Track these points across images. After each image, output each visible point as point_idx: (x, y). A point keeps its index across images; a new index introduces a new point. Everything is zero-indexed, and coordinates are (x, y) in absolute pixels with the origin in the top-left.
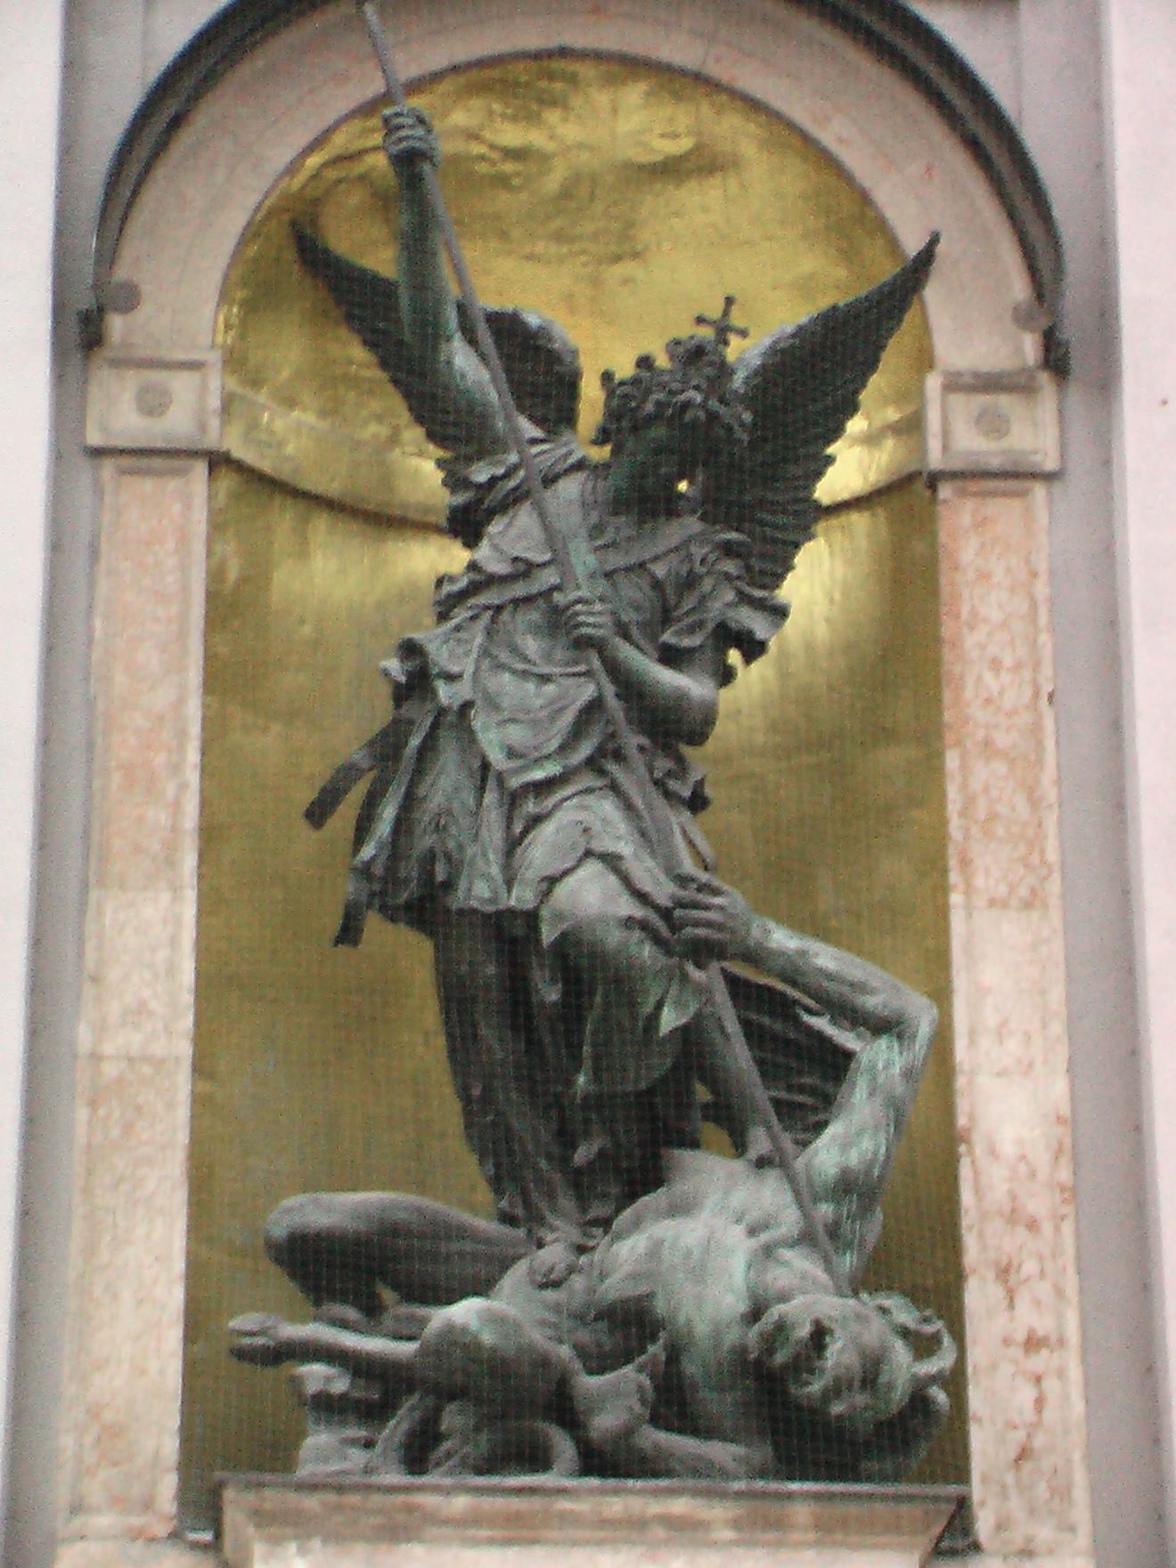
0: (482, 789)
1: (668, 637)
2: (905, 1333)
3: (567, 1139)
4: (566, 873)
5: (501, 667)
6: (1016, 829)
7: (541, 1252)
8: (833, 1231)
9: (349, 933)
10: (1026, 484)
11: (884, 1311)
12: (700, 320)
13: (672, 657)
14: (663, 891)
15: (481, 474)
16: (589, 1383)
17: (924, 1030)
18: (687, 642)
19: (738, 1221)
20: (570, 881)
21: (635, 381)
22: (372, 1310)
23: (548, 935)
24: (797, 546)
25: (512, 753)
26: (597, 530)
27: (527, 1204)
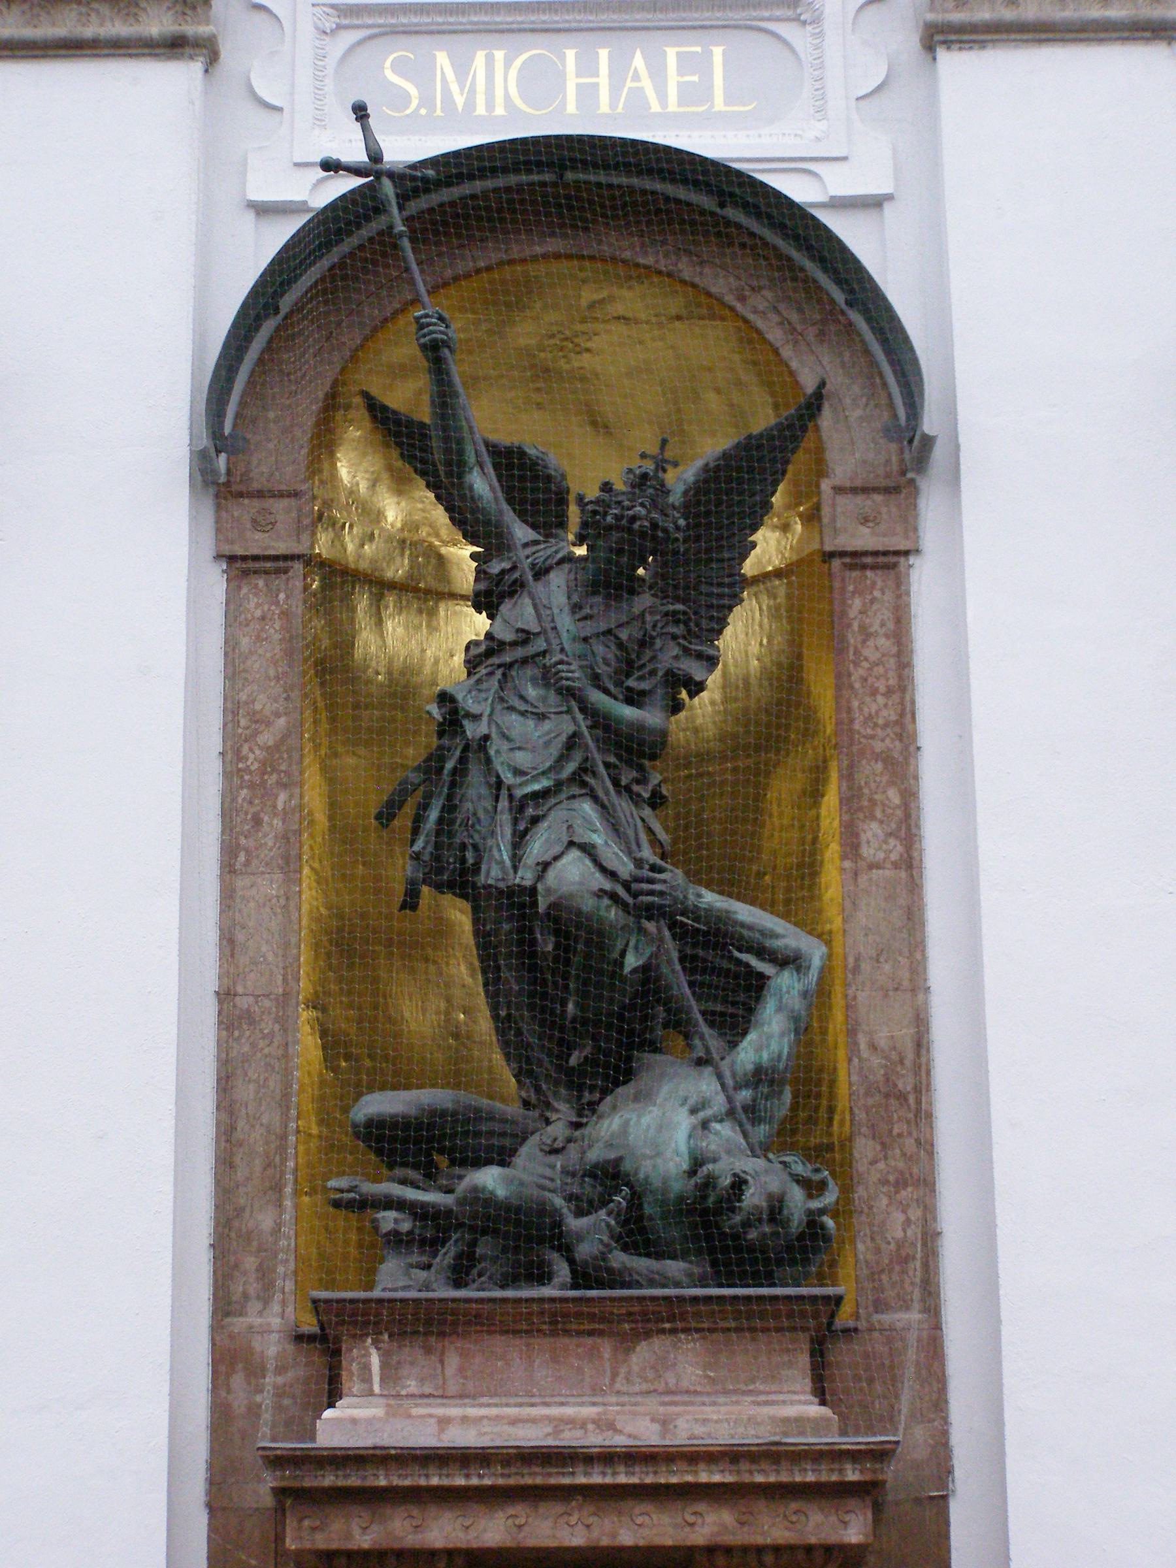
0: (497, 799)
1: (631, 683)
4: (556, 858)
5: (511, 709)
7: (549, 1129)
8: (751, 1109)
9: (411, 901)
10: (893, 559)
12: (643, 456)
13: (633, 698)
14: (626, 868)
16: (574, 1223)
17: (816, 962)
18: (644, 686)
19: (682, 1105)
20: (559, 864)
21: (597, 502)
22: (430, 1174)
23: (542, 905)
24: (730, 609)
26: (575, 608)
27: (538, 1090)
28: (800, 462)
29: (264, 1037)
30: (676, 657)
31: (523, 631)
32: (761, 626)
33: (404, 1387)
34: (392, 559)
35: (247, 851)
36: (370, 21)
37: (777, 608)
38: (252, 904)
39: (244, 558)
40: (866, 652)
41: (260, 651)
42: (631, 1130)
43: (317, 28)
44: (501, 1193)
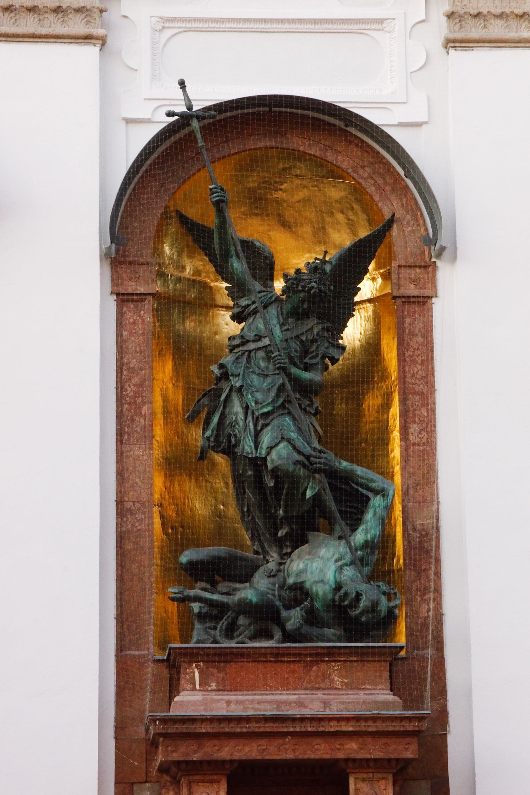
1: (307, 360)
2: (384, 593)
3: (275, 528)
6: (421, 419)
8: (362, 560)
11: (379, 586)
13: (307, 368)
14: (308, 450)
15: (244, 302)
16: (284, 613)
22: (214, 584)
23: (270, 466)
25: (256, 403)
27: (263, 547)
28: (381, 251)
29: (138, 521)
30: (327, 348)
31: (258, 335)
32: (361, 325)
33: (210, 686)
34: (189, 291)
35: (129, 435)
36: (179, 25)
37: (369, 318)
38: (131, 459)
39: (123, 294)
40: (411, 343)
41: (133, 339)
42: (308, 569)
43: (153, 29)
44: (254, 600)
